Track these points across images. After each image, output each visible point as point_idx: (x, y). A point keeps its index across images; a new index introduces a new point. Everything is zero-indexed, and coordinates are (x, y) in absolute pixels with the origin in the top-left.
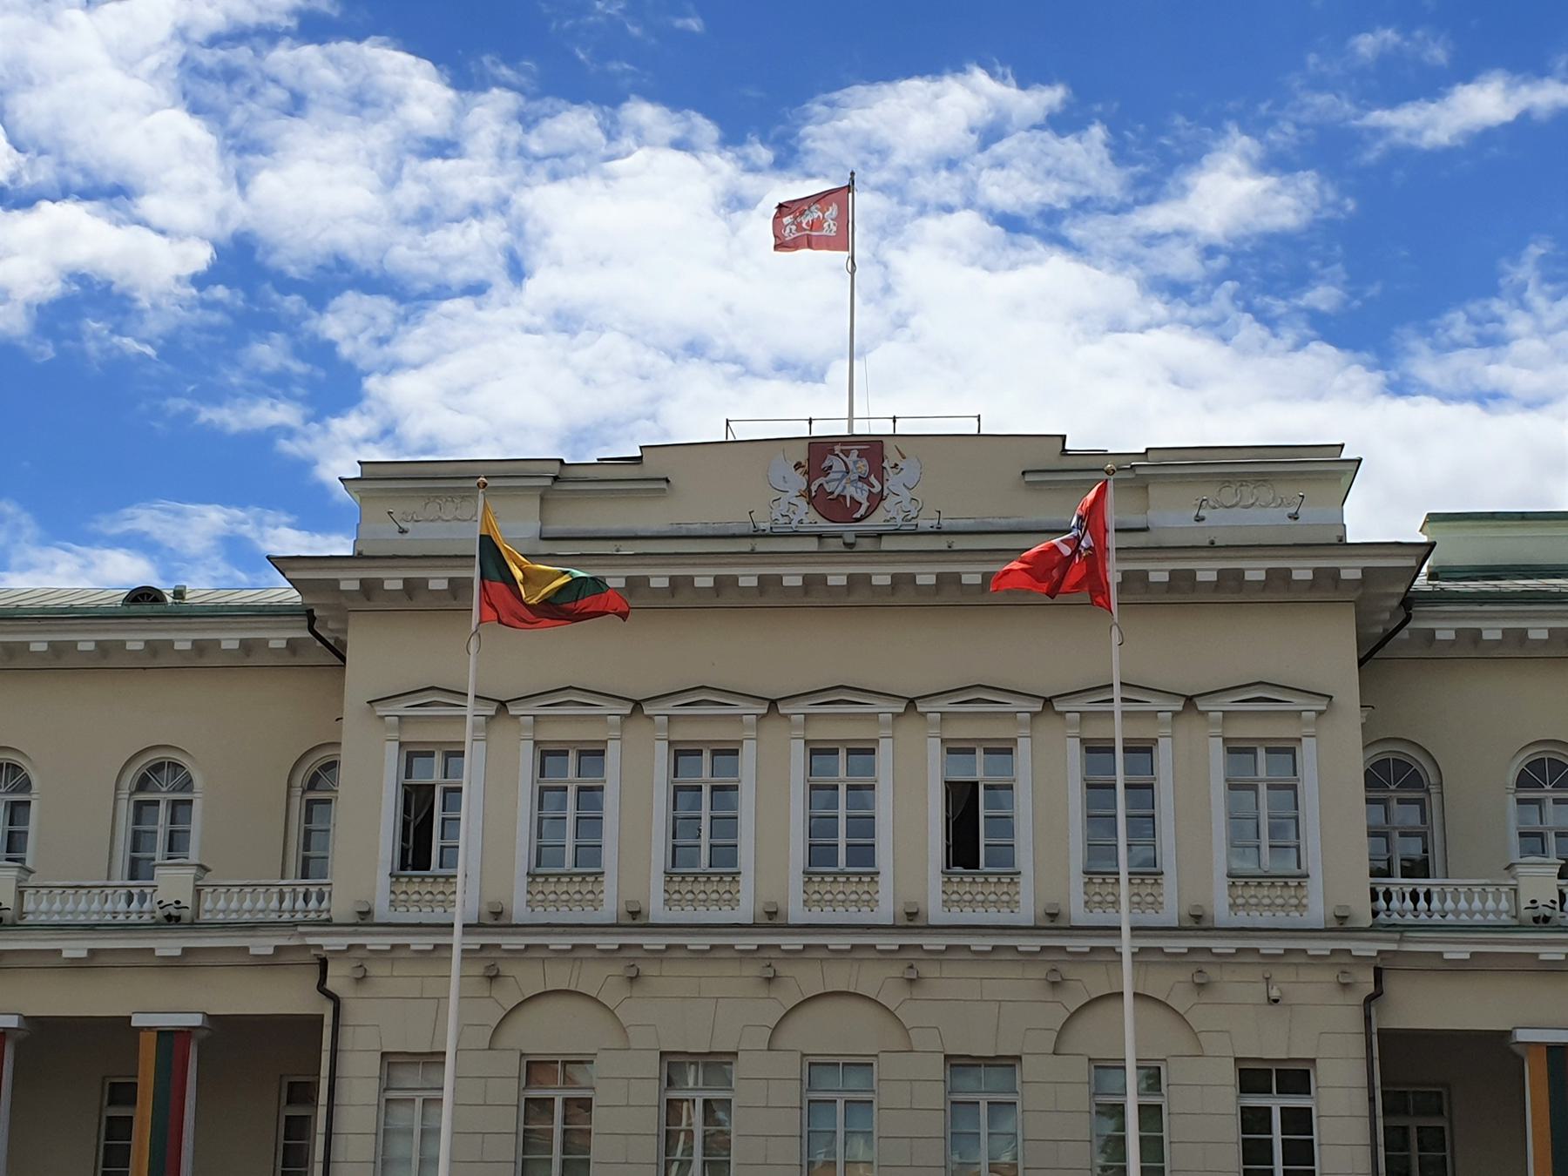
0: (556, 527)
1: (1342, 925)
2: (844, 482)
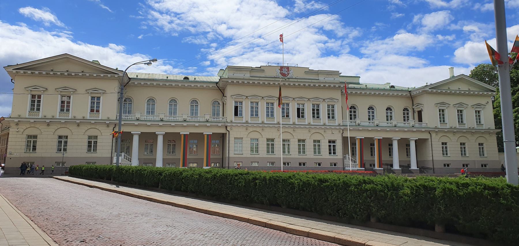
0: (252, 75)
1: (339, 125)
2: (285, 71)
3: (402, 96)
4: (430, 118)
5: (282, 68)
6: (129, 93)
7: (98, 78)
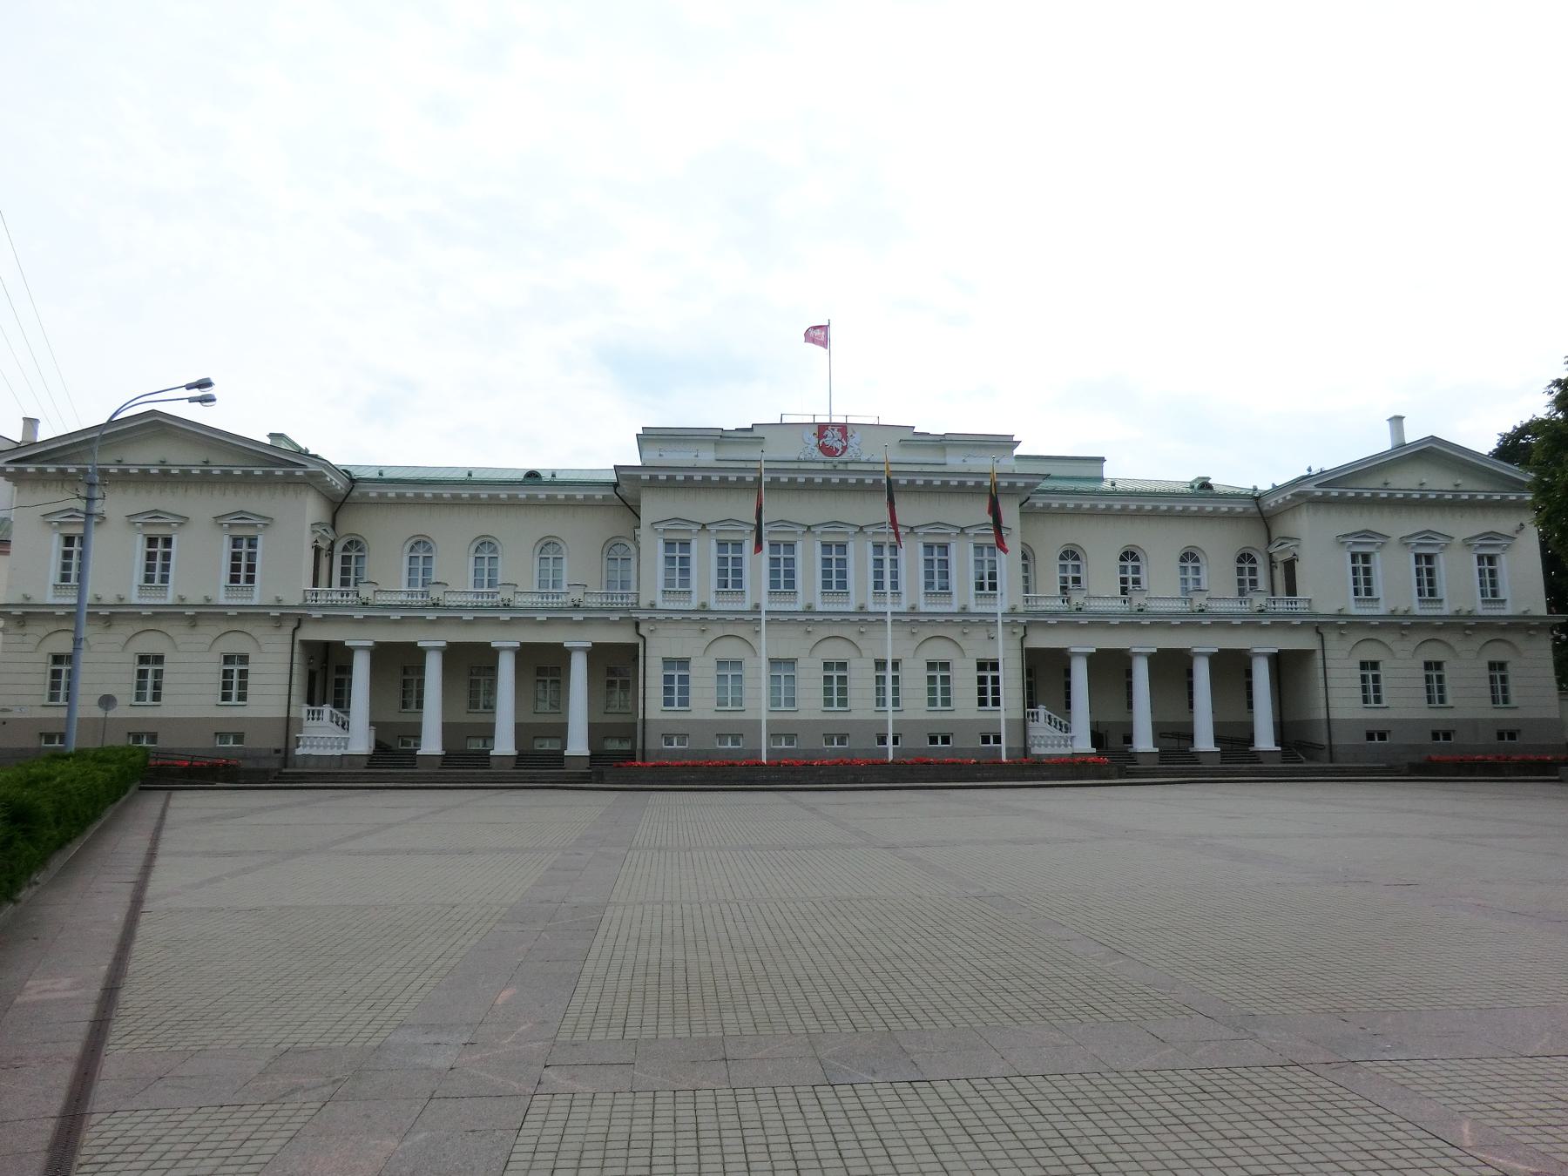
0: (721, 456)
2: (832, 440)
3: (1231, 517)
4: (1325, 585)
5: (822, 428)
6: (354, 524)
7: (247, 481)
